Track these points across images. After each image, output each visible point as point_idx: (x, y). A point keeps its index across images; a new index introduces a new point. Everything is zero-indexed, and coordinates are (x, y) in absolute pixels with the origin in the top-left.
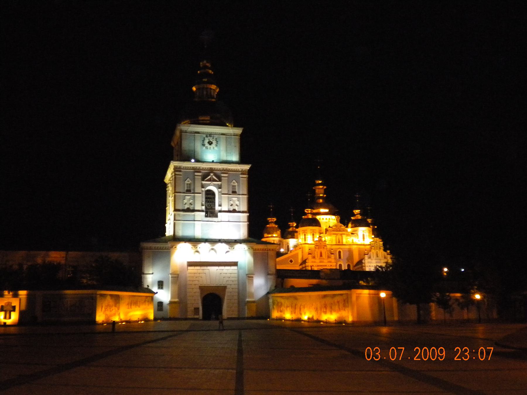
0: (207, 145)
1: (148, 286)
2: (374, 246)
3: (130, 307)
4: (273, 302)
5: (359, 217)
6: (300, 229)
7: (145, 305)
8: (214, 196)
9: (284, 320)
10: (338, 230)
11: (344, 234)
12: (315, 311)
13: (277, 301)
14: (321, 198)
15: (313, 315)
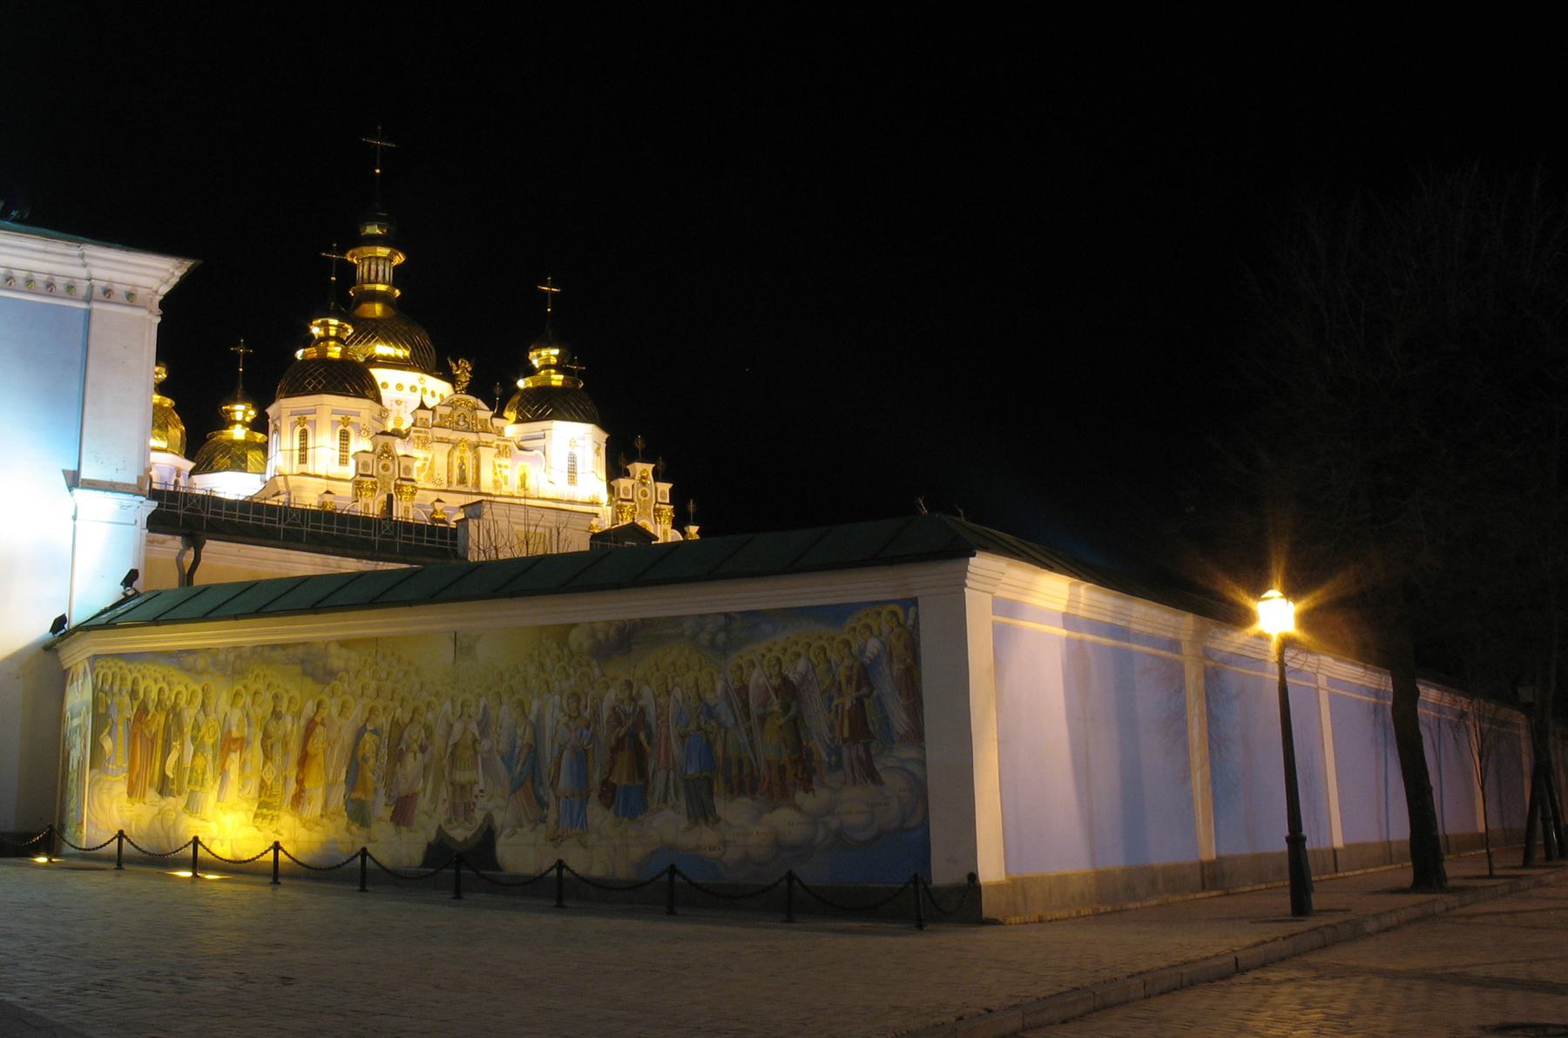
2: (632, 501)
4: (96, 701)
5: (557, 380)
6: (284, 409)
9: (195, 864)
10: (461, 423)
11: (487, 445)
12: (517, 786)
13: (133, 694)
14: (374, 297)
15: (489, 818)
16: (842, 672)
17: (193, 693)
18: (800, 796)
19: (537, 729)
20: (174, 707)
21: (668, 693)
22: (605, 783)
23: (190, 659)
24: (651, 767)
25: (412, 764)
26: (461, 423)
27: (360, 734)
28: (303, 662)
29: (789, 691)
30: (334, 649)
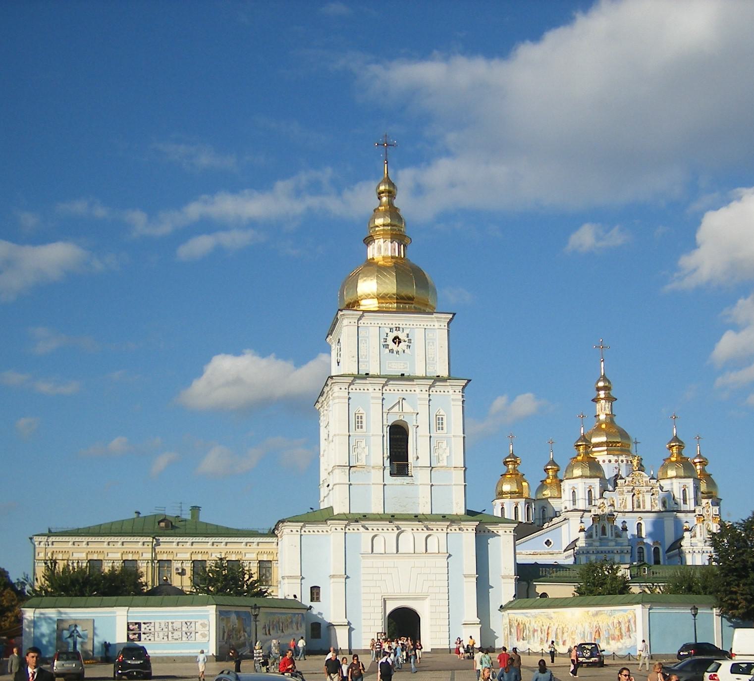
0: (392, 345)
1: (295, 596)
3: (267, 633)
4: (510, 622)
7: (293, 629)
8: (405, 437)
10: (637, 483)
13: (517, 621)
16: (626, 621)
17: (528, 621)
18: (621, 640)
19: (585, 630)
20: (524, 624)
21: (603, 623)
22: (595, 638)
23: (527, 614)
25: (565, 634)
26: (637, 483)
27: (557, 629)
28: (547, 615)
29: (619, 623)
30: (552, 613)
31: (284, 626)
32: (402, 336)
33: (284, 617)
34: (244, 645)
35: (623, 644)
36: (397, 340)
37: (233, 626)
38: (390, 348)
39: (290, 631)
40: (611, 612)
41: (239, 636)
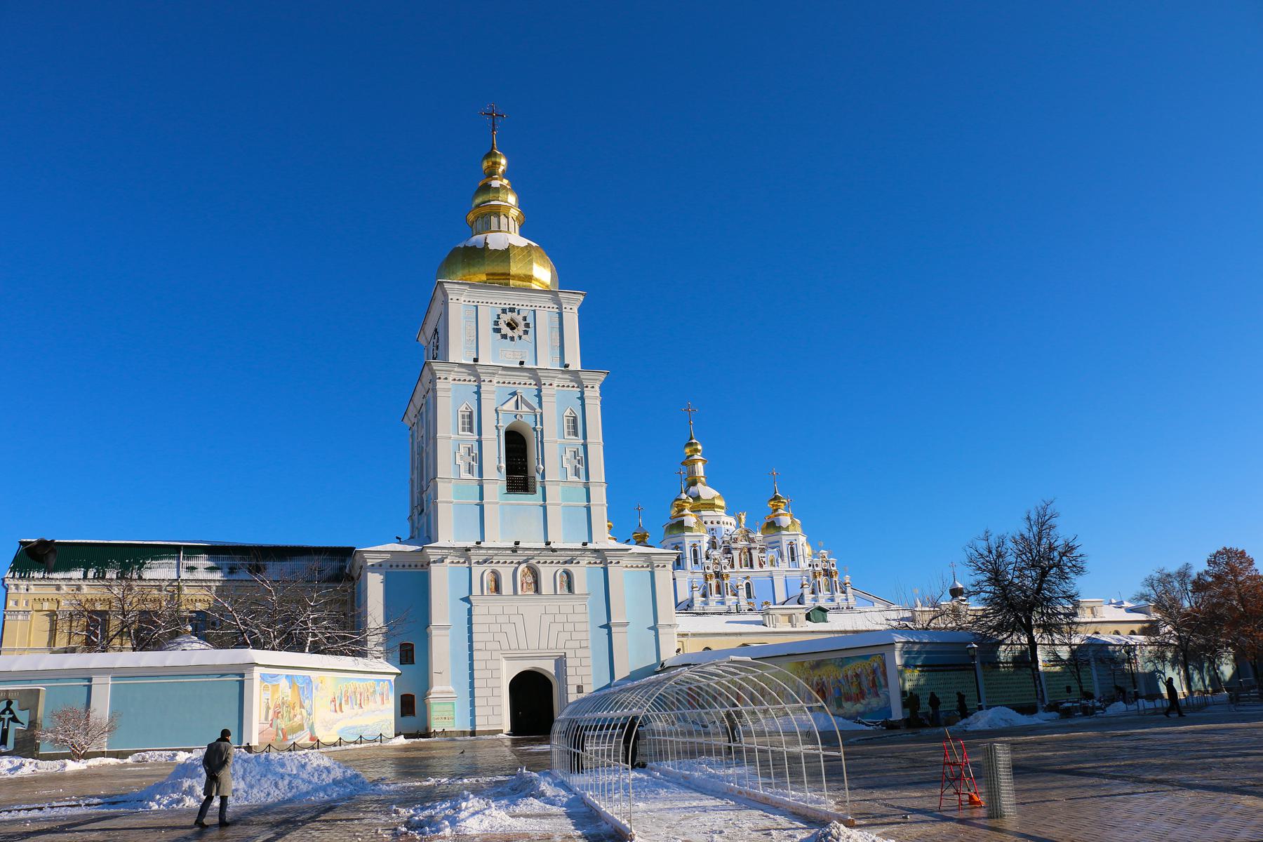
0: (506, 330)
3: (338, 709)
18: (862, 701)
24: (827, 694)
31: (362, 698)
32: (519, 319)
33: (362, 683)
34: (301, 728)
35: (866, 706)
36: (512, 326)
37: (283, 698)
38: (503, 332)
39: (371, 706)
40: (841, 661)
41: (292, 715)
